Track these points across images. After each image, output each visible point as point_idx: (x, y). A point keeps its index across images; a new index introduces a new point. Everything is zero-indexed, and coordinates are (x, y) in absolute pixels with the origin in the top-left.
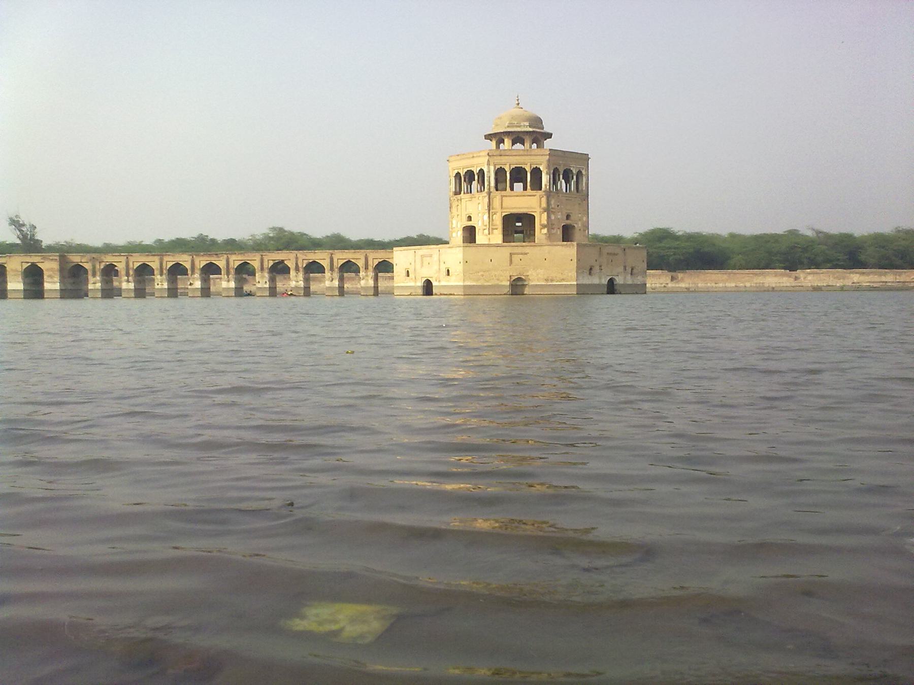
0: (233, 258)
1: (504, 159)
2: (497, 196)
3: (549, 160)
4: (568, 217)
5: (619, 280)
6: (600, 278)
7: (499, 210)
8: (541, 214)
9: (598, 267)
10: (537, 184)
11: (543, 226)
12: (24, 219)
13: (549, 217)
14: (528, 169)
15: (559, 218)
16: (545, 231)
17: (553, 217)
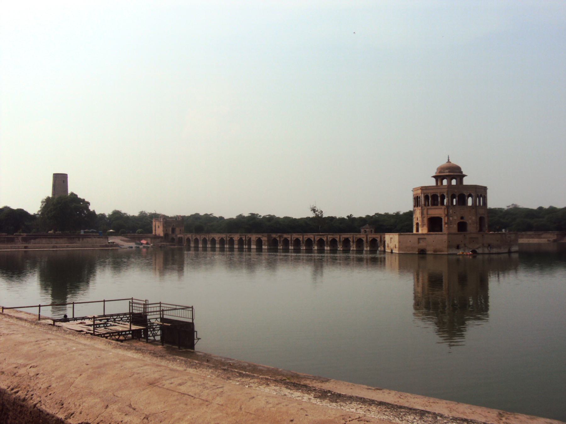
0: (329, 236)
1: (428, 191)
2: (425, 208)
3: (448, 191)
4: (462, 218)
5: (479, 251)
6: (464, 250)
7: (426, 216)
8: (445, 217)
9: (463, 245)
10: (442, 203)
11: (446, 223)
12: (318, 208)
13: (448, 218)
14: (439, 195)
15: (456, 219)
16: (446, 226)
17: (451, 218)
